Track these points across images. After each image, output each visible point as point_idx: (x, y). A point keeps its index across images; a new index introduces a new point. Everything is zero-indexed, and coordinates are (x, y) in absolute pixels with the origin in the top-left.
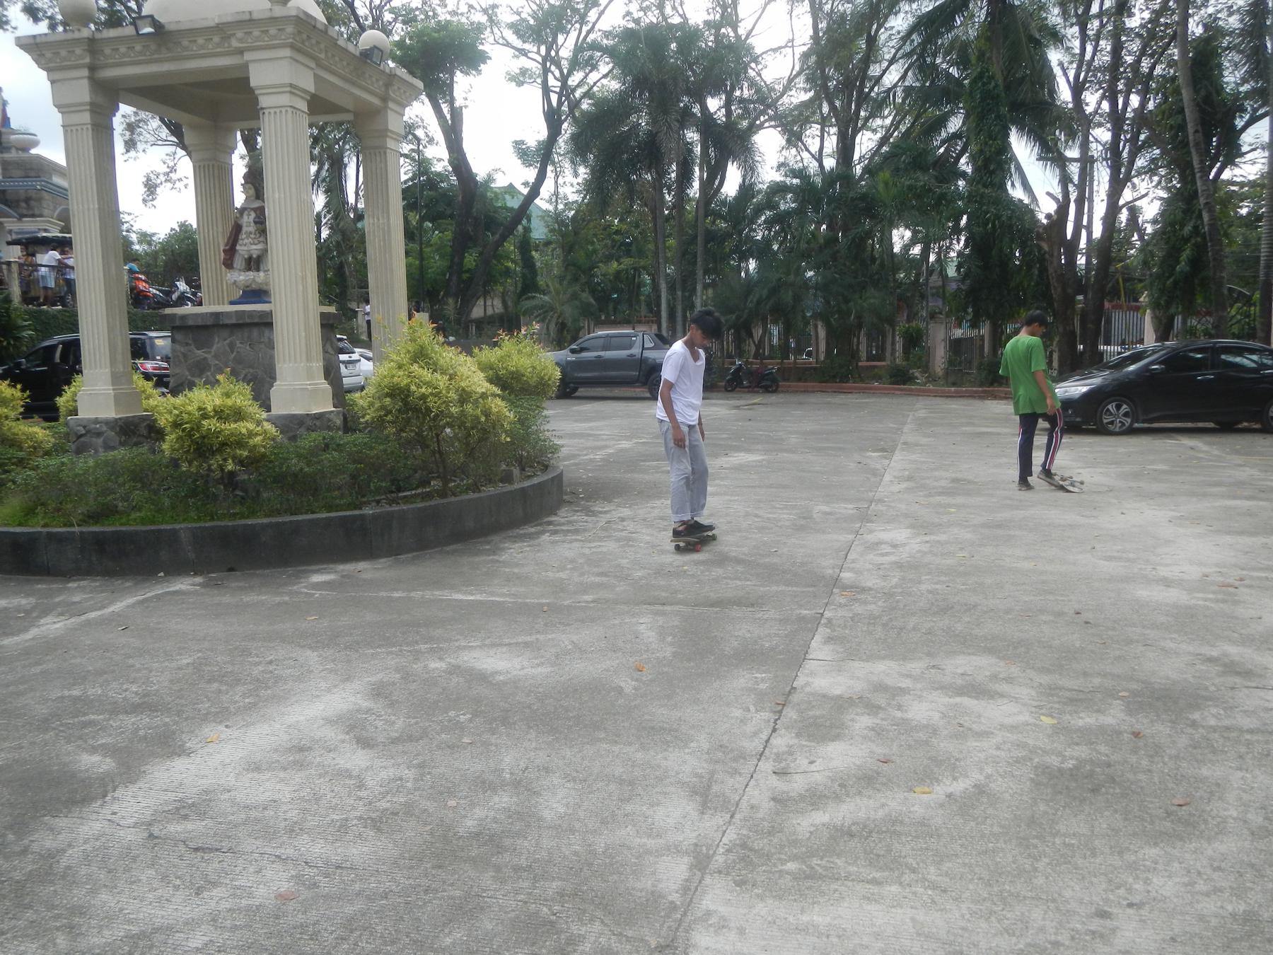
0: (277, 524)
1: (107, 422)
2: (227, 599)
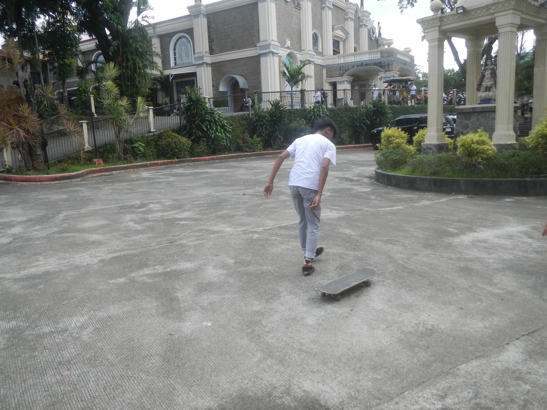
0: (494, 180)
1: (434, 145)
2: (477, 202)
